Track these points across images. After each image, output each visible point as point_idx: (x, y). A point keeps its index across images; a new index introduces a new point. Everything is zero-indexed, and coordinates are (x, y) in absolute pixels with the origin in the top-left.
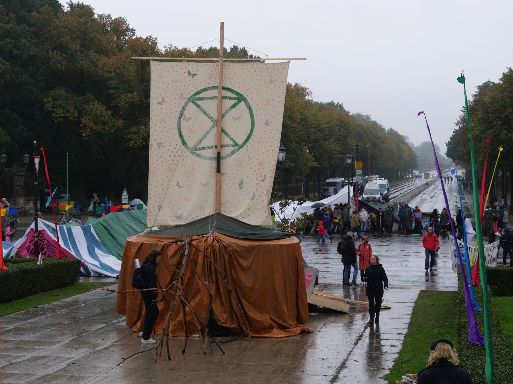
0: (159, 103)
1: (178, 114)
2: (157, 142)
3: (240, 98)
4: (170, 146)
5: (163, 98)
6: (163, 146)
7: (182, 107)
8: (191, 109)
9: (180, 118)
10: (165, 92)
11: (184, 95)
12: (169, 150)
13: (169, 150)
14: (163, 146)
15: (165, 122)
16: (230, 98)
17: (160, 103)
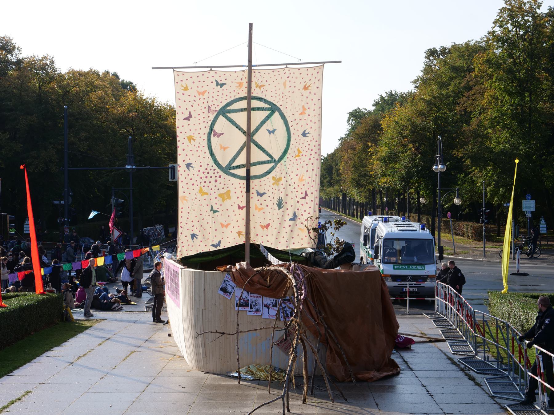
0: (185, 119)
1: (207, 130)
3: (273, 108)
6: (192, 167)
8: (222, 124)
9: (210, 134)
11: (213, 108)
14: (192, 167)
15: (194, 140)
16: (263, 109)
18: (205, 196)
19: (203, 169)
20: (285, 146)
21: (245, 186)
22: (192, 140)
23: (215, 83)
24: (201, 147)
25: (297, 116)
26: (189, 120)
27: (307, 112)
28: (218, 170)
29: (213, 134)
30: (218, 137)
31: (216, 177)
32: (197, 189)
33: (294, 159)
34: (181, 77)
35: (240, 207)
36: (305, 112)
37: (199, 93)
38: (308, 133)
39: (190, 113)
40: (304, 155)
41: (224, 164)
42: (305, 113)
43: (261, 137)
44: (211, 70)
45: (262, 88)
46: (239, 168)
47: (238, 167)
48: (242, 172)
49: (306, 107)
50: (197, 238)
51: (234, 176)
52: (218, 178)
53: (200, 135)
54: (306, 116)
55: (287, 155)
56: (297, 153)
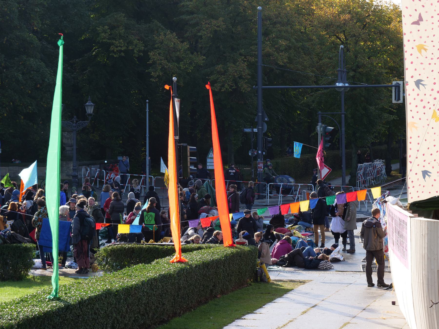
0: (414, 23)
2: (415, 79)
4: (435, 84)
6: (423, 85)
10: (423, 6)
12: (432, 90)
13: (432, 90)
14: (423, 85)
15: (425, 50)
17: (416, 23)
22: (423, 51)
26: (419, 24)
50: (429, 176)
53: (433, 44)
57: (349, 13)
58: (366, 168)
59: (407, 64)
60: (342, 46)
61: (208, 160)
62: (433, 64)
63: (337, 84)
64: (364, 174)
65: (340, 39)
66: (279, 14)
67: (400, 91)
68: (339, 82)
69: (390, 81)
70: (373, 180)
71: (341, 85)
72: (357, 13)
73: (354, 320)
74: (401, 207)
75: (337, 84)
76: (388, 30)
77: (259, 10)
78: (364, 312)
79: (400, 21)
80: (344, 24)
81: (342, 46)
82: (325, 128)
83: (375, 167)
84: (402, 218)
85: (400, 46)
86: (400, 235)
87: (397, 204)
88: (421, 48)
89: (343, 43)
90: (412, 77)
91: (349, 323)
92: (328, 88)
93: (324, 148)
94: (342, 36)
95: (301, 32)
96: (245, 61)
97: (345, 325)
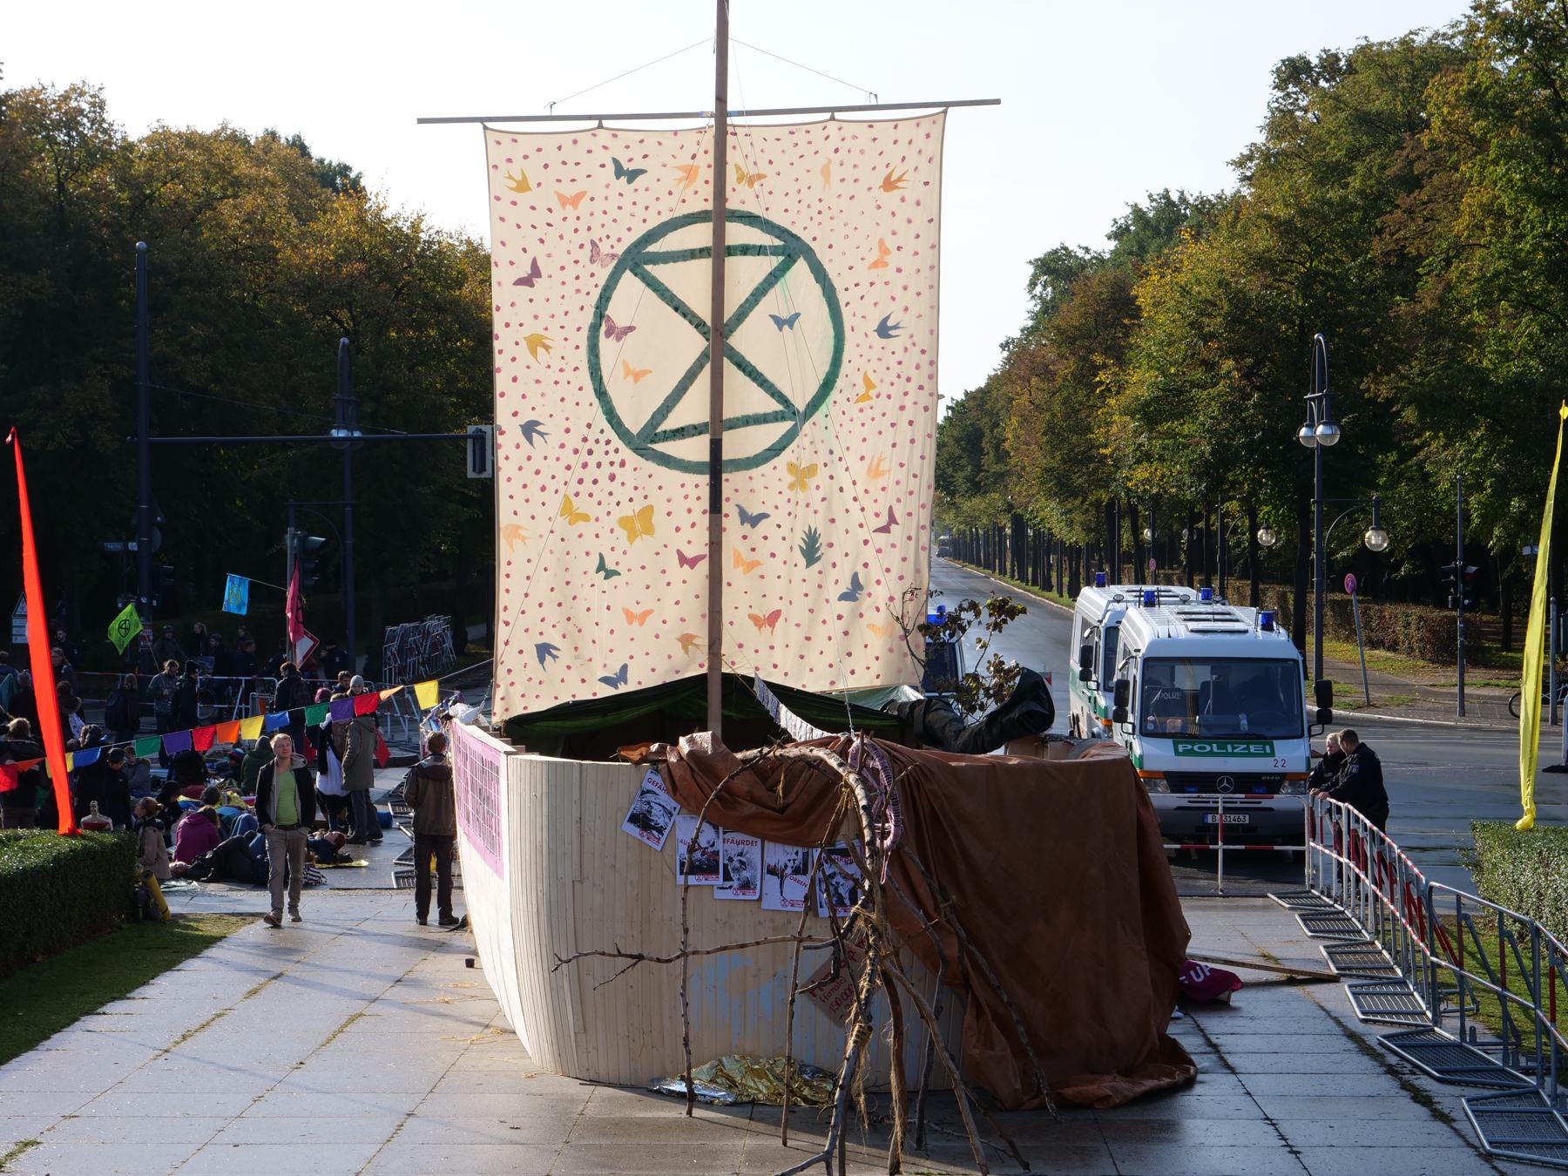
1: (588, 317)
2: (524, 418)
3: (792, 249)
5: (534, 263)
6: (541, 434)
7: (599, 290)
8: (631, 294)
9: (595, 328)
10: (542, 241)
11: (605, 248)
13: (562, 446)
14: (541, 434)
15: (547, 348)
16: (760, 250)
18: (581, 526)
19: (573, 441)
20: (826, 368)
21: (705, 492)
22: (540, 350)
23: (611, 167)
24: (569, 369)
25: (863, 274)
26: (532, 285)
27: (894, 259)
28: (617, 442)
29: (603, 328)
30: (619, 339)
31: (612, 464)
32: (555, 503)
33: (852, 409)
34: (508, 149)
35: (683, 560)
36: (887, 259)
37: (564, 201)
38: (896, 327)
39: (534, 262)
40: (883, 397)
41: (634, 424)
42: (886, 264)
43: (749, 339)
44: (600, 126)
45: (757, 185)
46: (683, 437)
47: (680, 433)
48: (696, 449)
49: (891, 243)
50: (555, 657)
51: (666, 461)
52: (616, 469)
53: (564, 333)
54: (888, 274)
55: (834, 395)
56: (861, 389)
57: (363, 260)
58: (405, 635)
59: (501, 382)
60: (344, 340)
61: (16, 622)
62: (563, 383)
63: (334, 433)
64: (400, 650)
65: (341, 323)
66: (190, 260)
67: (484, 448)
68: (338, 428)
69: (463, 427)
70: (423, 664)
71: (342, 434)
72: (380, 261)
73: (375, 1008)
74: (485, 729)
75: (334, 433)
76: (455, 302)
77: (139, 251)
78: (398, 988)
79: (486, 281)
80: (351, 286)
81: (344, 340)
82: (303, 540)
83: (426, 634)
84: (489, 757)
85: (484, 338)
86: (486, 799)
87: (476, 722)
88: (536, 344)
89: (346, 333)
90: (515, 414)
91: (361, 1015)
92: (310, 442)
93: (302, 590)
94: (344, 315)
95: (245, 307)
96: (103, 376)
97: (352, 1020)
